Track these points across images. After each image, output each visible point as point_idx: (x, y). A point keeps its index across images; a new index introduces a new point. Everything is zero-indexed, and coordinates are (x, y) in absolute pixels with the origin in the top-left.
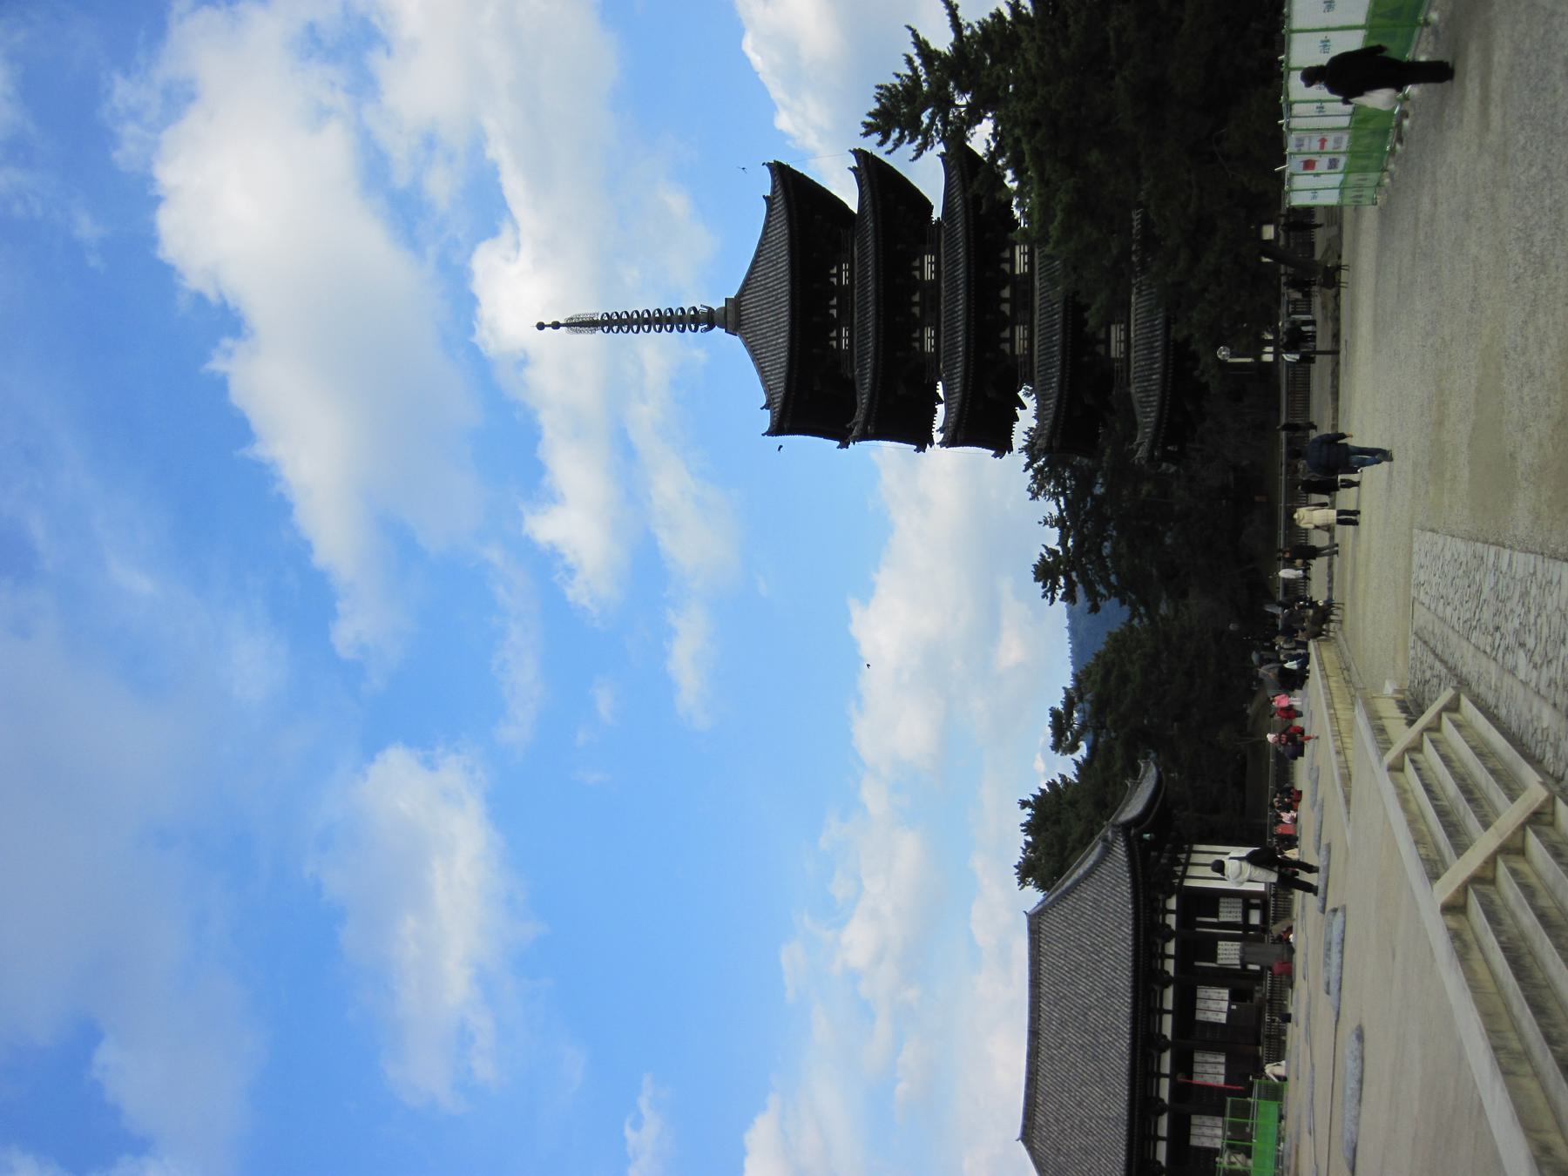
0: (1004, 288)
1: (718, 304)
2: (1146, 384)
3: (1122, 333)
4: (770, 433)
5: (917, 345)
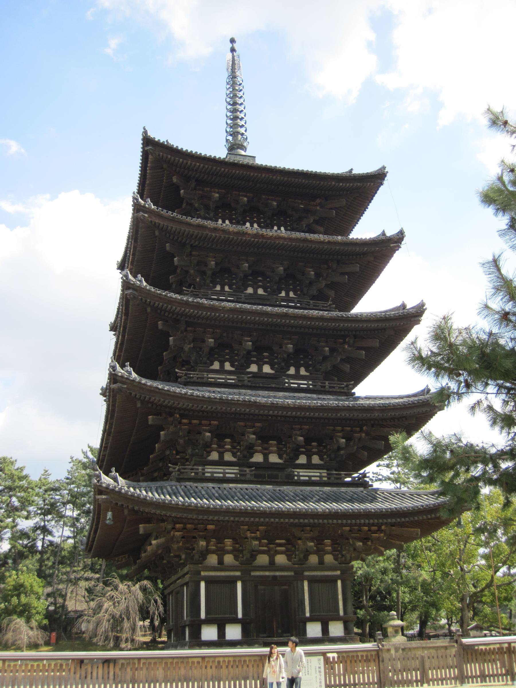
0: (272, 369)
1: (248, 153)
2: (182, 493)
3: (233, 476)
4: (145, 132)
5: (218, 288)
